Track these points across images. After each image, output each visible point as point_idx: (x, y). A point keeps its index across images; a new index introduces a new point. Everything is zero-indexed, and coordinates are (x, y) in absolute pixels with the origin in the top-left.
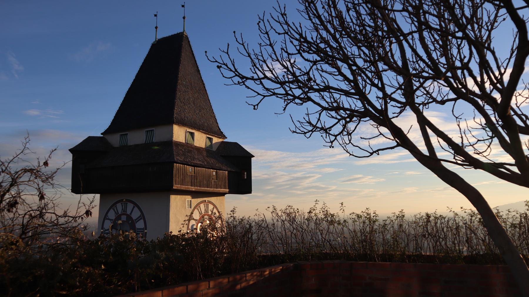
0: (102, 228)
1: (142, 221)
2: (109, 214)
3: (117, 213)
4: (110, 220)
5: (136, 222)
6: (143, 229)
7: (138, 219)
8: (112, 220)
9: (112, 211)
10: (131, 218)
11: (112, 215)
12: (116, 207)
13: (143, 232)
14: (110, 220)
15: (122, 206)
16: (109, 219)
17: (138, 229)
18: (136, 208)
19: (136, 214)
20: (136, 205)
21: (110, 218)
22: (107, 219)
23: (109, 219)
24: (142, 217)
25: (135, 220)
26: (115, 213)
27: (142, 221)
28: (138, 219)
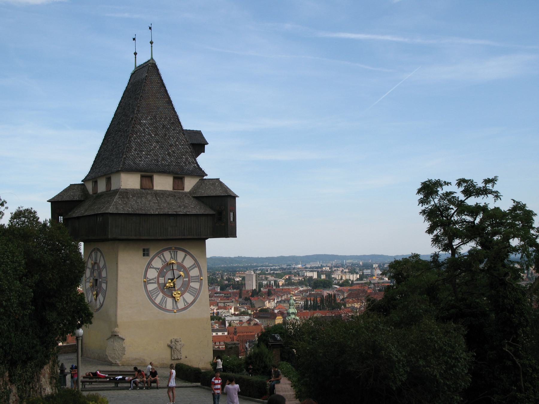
1: (196, 270)
2: (153, 263)
3: (164, 261)
4: (156, 269)
8: (158, 269)
9: (157, 258)
11: (158, 263)
12: (163, 255)
14: (156, 269)
15: (171, 254)
17: (192, 277)
18: (188, 257)
20: (187, 253)
21: (155, 266)
23: (153, 268)
25: (189, 268)
27: (196, 270)
28: (192, 268)
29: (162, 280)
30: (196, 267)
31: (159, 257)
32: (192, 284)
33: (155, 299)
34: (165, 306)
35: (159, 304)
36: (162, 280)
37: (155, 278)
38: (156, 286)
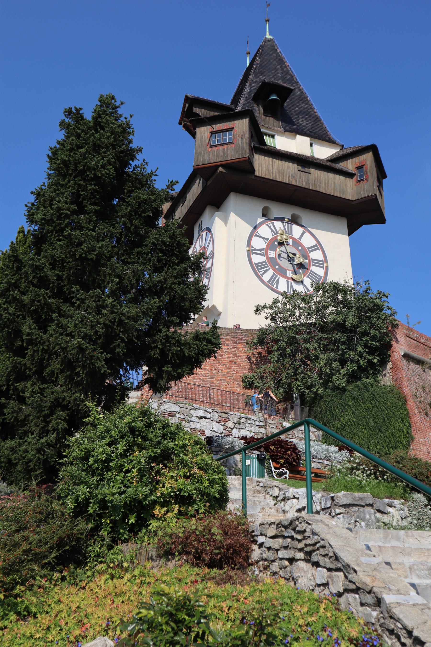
0: (249, 244)
4: (263, 238)
5: (310, 252)
6: (322, 261)
7: (314, 248)
10: (301, 245)
12: (273, 224)
13: (323, 264)
14: (263, 238)
16: (260, 237)
17: (313, 260)
18: (307, 235)
19: (308, 241)
22: (256, 235)
23: (260, 237)
24: (319, 246)
26: (272, 231)
28: (314, 248)
29: (272, 254)
30: (318, 249)
31: (267, 225)
32: (314, 269)
33: (262, 275)
34: (277, 287)
35: (269, 281)
36: (272, 254)
37: (263, 249)
38: (263, 259)
